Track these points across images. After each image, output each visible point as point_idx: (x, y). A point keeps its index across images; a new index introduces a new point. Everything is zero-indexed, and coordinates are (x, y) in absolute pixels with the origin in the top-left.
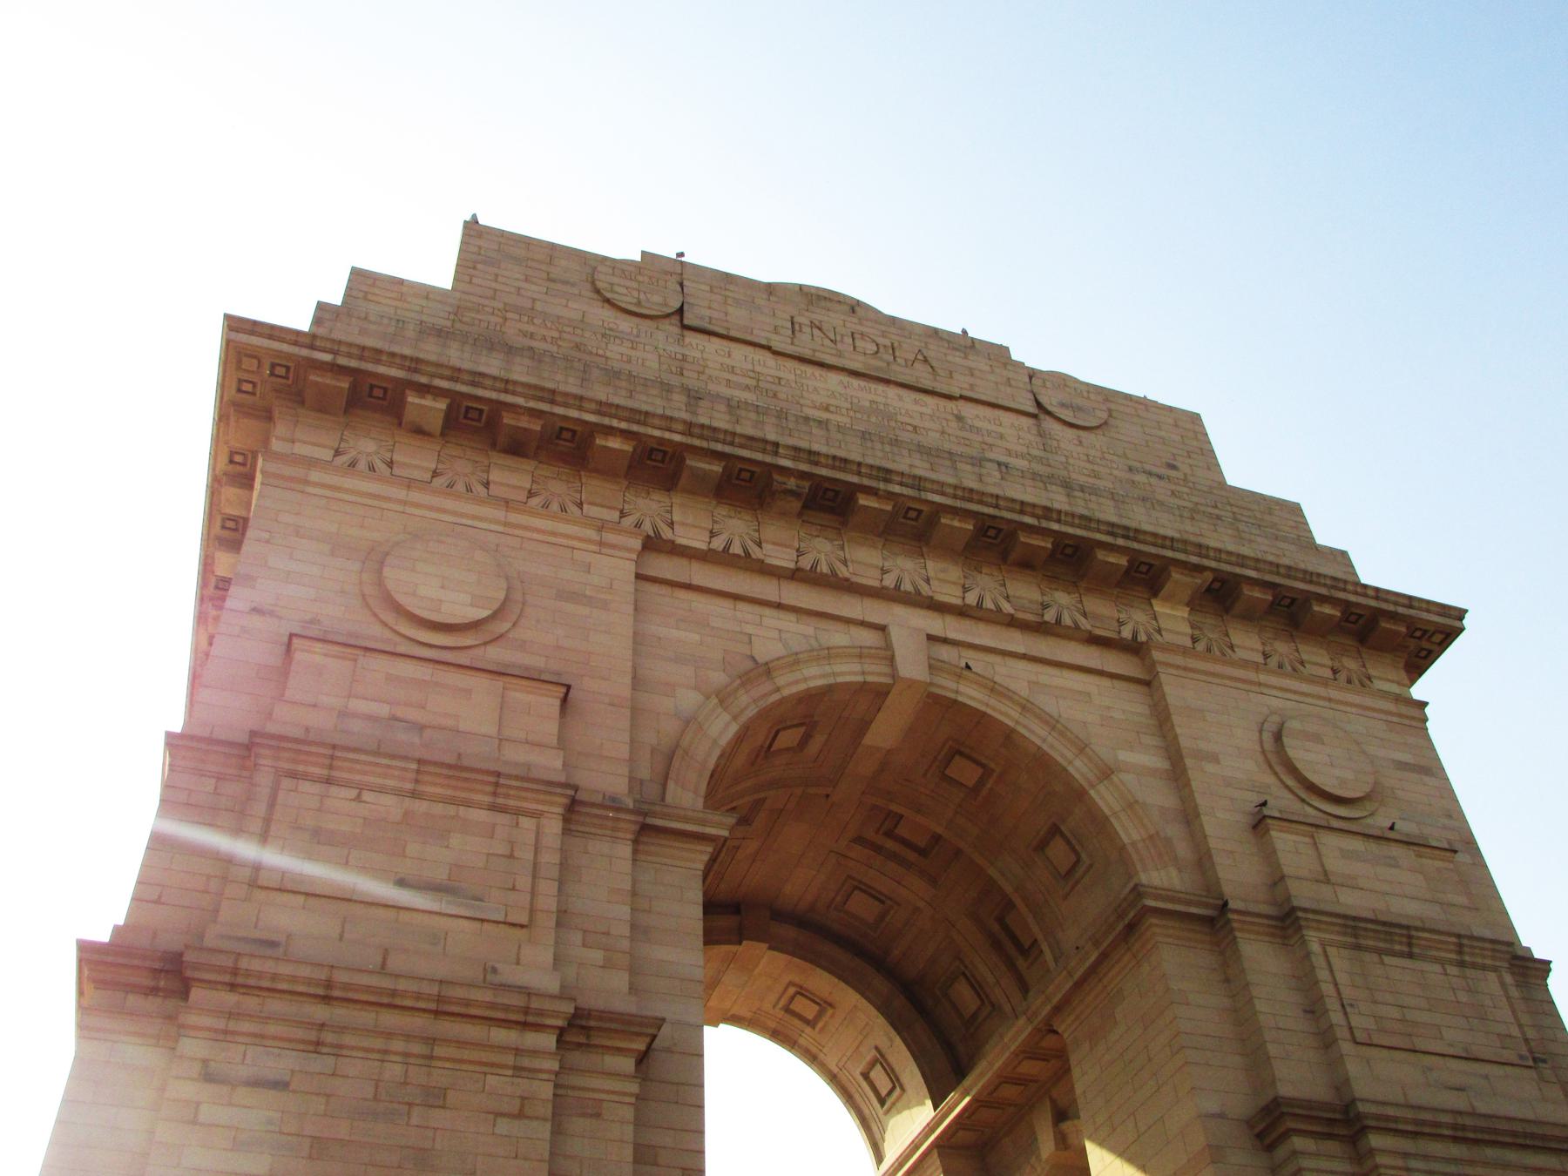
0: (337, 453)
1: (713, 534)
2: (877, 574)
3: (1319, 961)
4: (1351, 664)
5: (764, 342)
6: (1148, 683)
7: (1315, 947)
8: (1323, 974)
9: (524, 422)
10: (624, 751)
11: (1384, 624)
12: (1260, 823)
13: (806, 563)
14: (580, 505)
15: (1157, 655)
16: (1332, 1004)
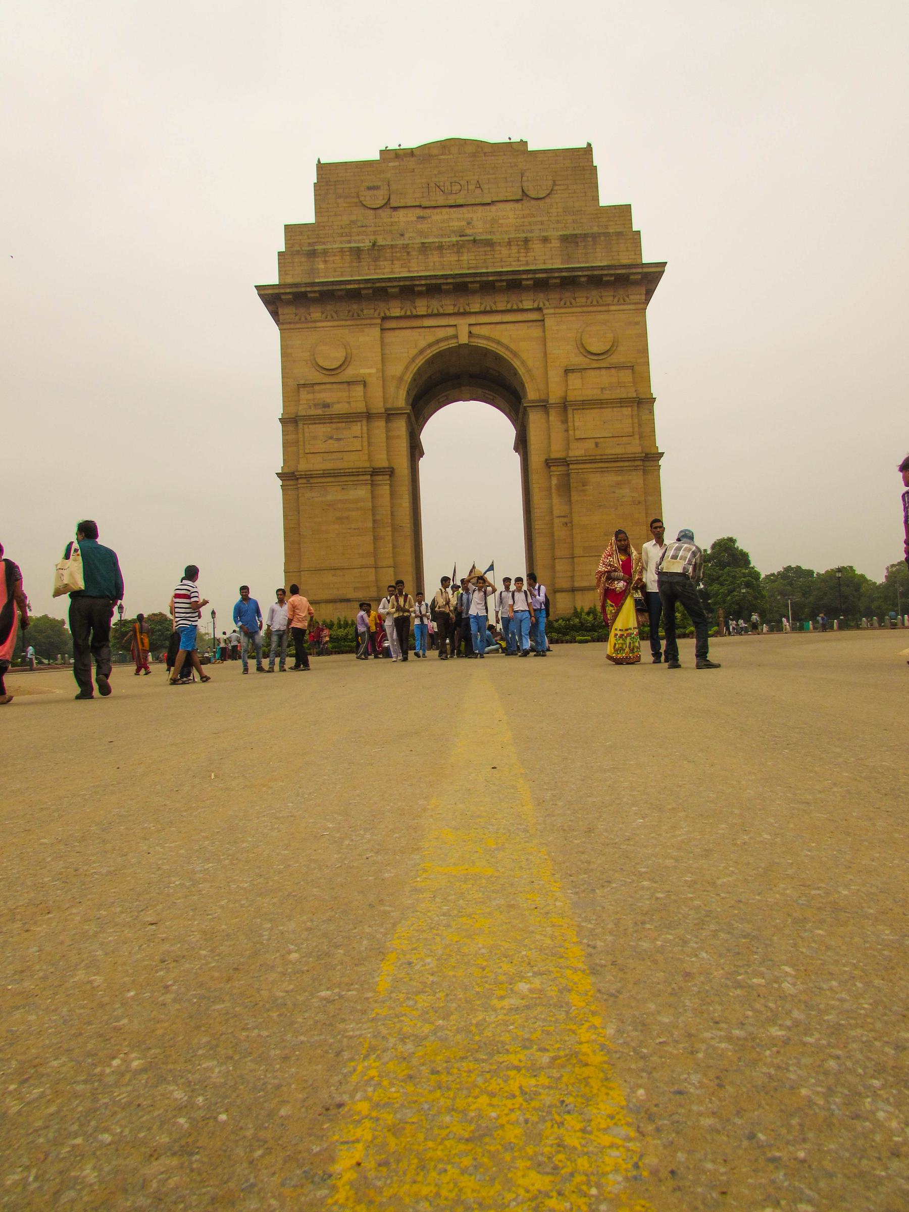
0: (296, 315)
1: (402, 309)
2: (452, 307)
3: (570, 416)
4: (621, 292)
5: (418, 204)
6: (543, 320)
7: (570, 411)
8: (570, 420)
9: (339, 293)
10: (382, 395)
11: (632, 277)
12: (567, 371)
13: (430, 312)
14: (362, 311)
15: (545, 311)
16: (571, 428)
